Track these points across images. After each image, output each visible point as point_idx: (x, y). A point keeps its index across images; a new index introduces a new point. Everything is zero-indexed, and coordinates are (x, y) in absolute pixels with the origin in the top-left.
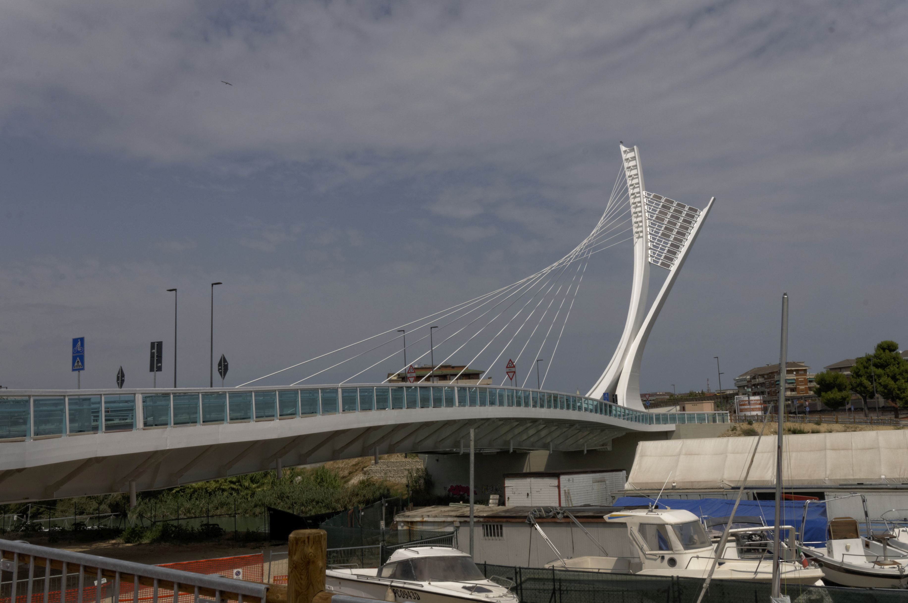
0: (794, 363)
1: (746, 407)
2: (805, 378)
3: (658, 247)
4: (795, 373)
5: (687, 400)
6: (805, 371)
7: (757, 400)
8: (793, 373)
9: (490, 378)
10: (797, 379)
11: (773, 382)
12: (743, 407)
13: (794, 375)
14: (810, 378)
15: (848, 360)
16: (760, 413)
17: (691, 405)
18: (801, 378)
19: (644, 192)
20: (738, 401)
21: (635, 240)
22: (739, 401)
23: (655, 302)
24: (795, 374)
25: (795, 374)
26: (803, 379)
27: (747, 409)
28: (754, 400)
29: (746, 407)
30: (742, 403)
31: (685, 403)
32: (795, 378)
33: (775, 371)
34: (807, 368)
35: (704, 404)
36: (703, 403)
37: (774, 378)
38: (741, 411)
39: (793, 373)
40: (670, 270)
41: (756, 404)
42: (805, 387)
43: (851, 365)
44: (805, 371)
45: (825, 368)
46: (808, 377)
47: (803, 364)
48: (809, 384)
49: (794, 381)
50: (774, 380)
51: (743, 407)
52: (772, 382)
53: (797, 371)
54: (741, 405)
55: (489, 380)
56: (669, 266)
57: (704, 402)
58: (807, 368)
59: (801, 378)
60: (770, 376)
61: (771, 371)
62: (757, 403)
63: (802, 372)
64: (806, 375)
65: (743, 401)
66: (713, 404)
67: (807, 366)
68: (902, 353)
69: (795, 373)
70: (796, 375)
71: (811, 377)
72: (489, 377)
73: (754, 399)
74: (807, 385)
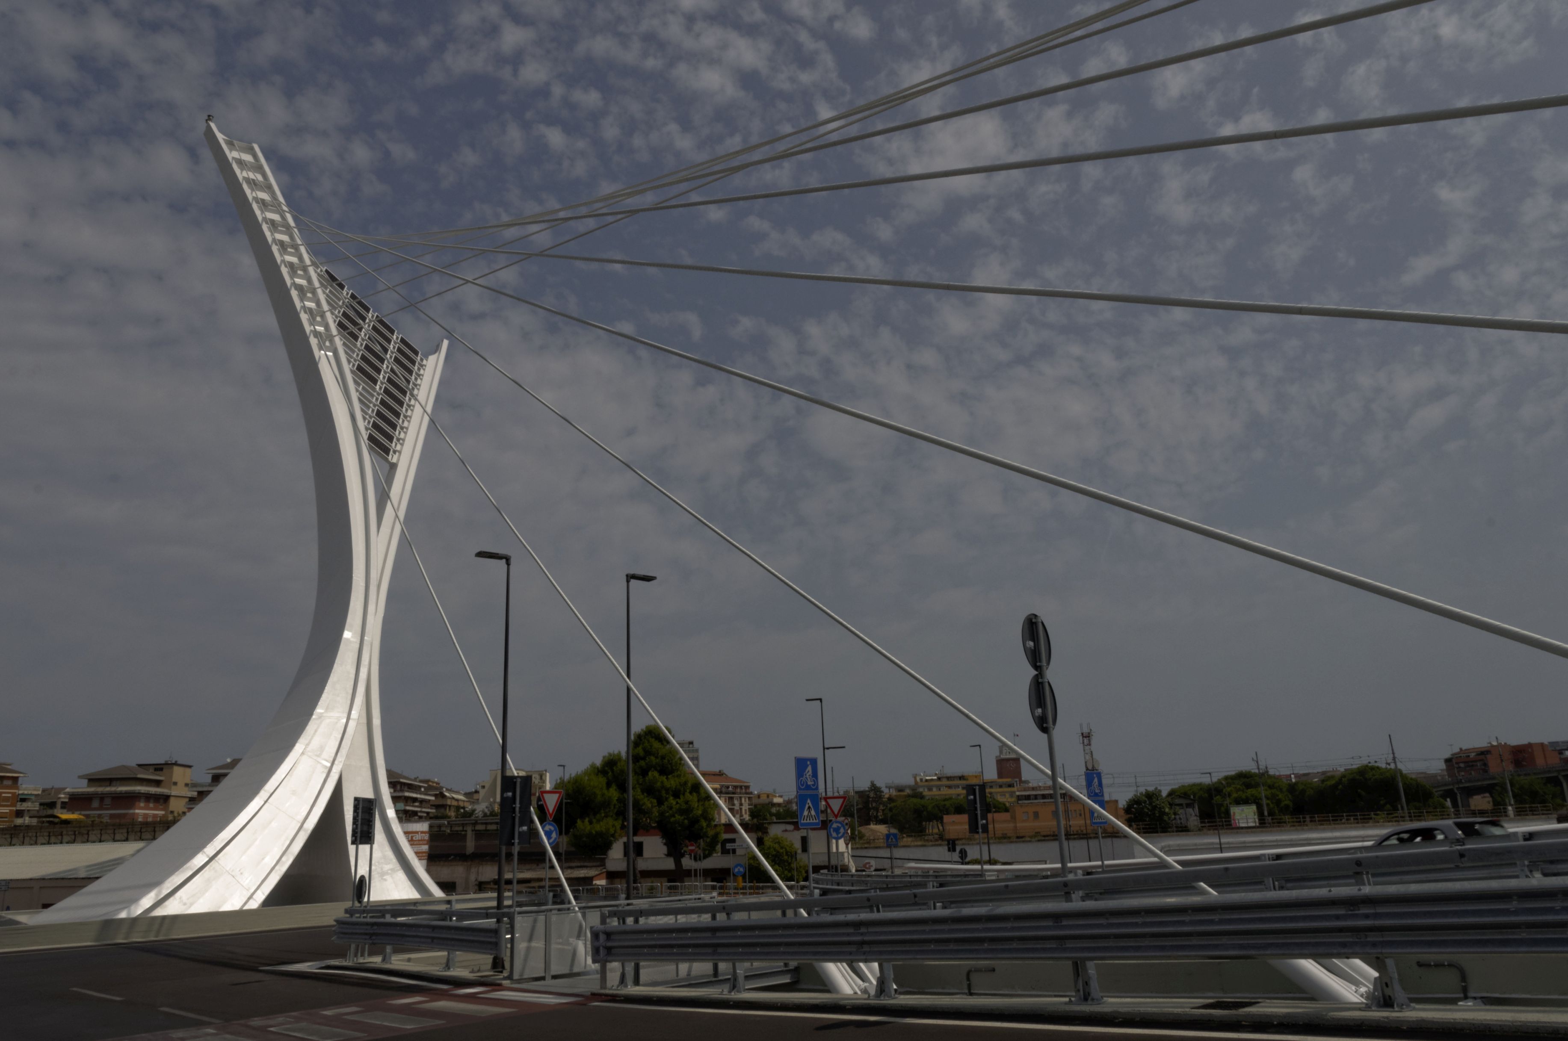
2: (13, 794)
6: (16, 779)
14: (23, 794)
26: (10, 795)
28: (422, 832)
34: (21, 775)
42: (10, 810)
43: (134, 776)
44: (16, 779)
45: (80, 777)
46: (21, 792)
62: (424, 840)
63: (9, 783)
64: (17, 788)
71: (26, 792)
73: (421, 830)
74: (15, 806)
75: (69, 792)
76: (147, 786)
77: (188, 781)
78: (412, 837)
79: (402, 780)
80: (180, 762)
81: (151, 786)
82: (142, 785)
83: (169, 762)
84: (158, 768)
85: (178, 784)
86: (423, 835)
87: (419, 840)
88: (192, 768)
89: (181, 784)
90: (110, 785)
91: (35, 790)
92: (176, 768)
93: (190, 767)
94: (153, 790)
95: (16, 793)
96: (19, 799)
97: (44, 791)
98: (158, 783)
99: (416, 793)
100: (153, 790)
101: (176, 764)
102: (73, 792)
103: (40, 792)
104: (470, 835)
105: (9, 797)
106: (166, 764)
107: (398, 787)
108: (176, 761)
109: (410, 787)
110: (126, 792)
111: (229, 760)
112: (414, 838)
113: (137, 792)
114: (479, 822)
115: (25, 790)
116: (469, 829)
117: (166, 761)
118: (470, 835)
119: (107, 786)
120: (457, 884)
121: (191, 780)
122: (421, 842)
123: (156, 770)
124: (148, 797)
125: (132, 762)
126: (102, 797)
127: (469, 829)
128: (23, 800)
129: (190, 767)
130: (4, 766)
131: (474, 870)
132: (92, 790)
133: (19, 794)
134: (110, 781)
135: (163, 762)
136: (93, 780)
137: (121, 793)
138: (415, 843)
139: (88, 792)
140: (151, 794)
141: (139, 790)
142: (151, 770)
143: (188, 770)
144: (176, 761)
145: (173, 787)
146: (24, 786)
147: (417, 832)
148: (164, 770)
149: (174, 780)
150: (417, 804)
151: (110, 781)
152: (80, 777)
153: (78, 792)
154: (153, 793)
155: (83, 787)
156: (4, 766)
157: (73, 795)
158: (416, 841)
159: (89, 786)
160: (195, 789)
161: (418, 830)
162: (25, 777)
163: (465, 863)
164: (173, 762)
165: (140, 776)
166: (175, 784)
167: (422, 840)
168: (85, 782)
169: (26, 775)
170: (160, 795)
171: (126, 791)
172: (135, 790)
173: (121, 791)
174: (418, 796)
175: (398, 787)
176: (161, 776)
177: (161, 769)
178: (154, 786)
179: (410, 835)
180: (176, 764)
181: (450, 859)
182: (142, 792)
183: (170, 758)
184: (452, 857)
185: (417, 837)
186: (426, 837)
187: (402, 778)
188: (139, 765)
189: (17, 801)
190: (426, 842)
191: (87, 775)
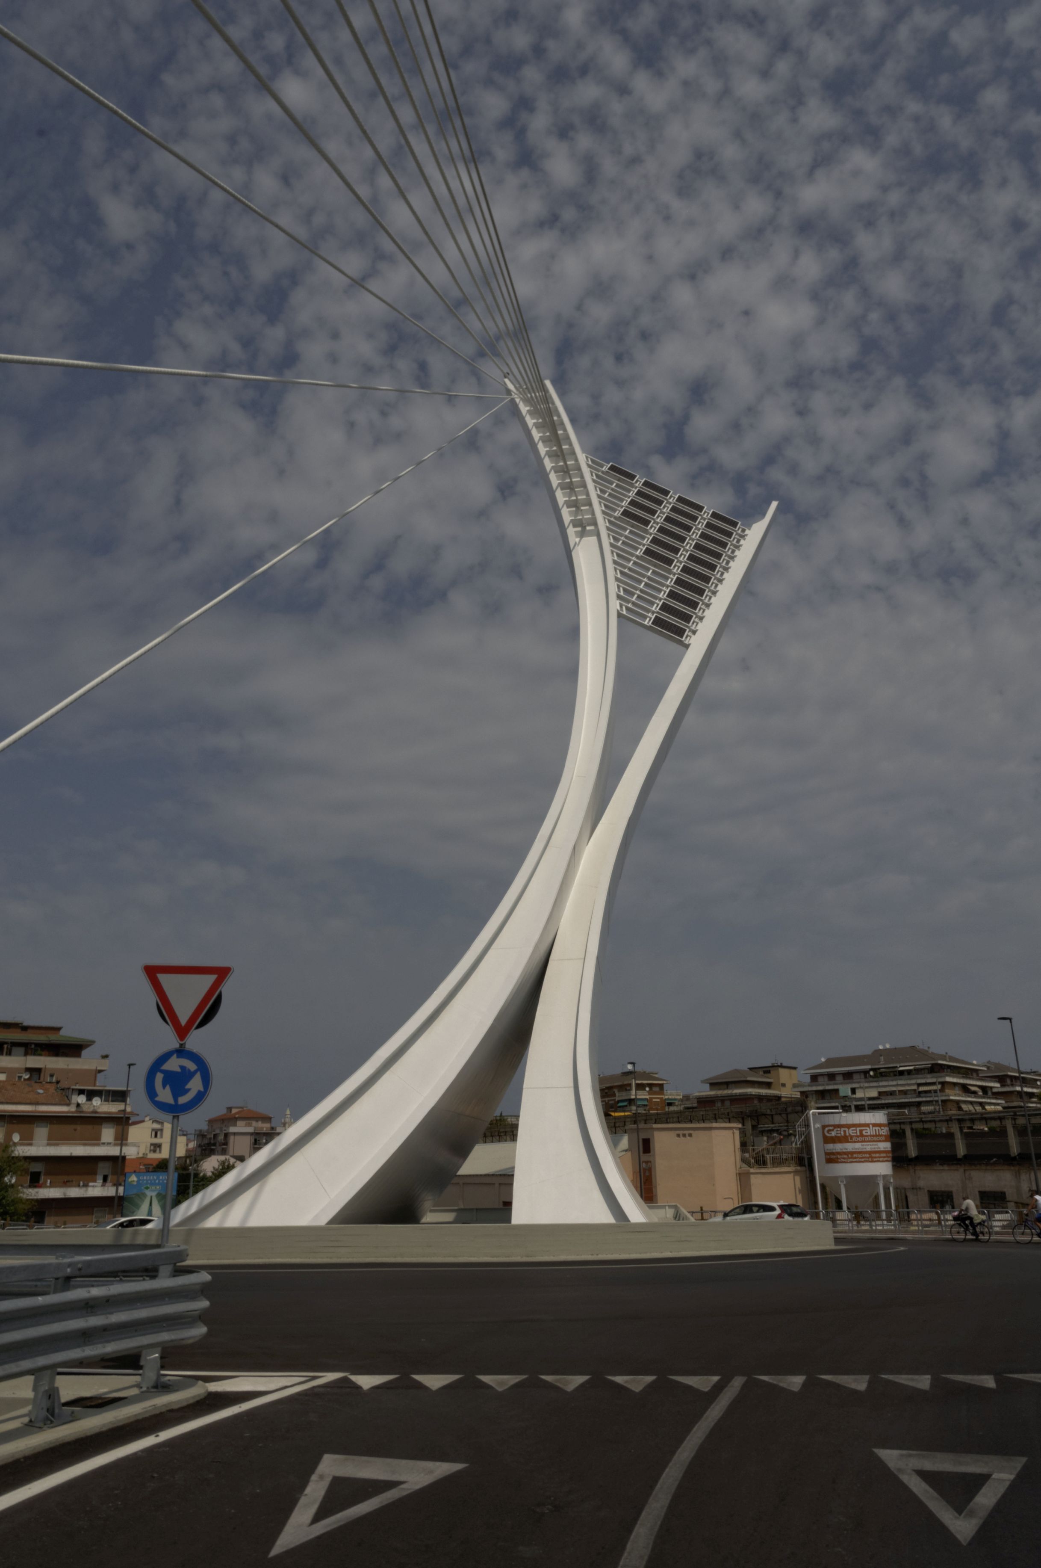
0: (645, 1072)
1: (850, 1147)
2: (661, 1099)
3: (640, 582)
4: (647, 1089)
5: (658, 1119)
6: (661, 1086)
7: (880, 1125)
8: (645, 1090)
9: (105, 1057)
10: (651, 1098)
11: (613, 1102)
12: (838, 1147)
13: (645, 1093)
15: (737, 1071)
16: (882, 1169)
17: (673, 1134)
18: (656, 1098)
19: (584, 455)
20: (818, 1126)
21: (573, 539)
22: (824, 1127)
23: (655, 719)
24: (648, 1092)
25: (648, 1092)
26: (659, 1100)
27: (852, 1153)
28: (875, 1125)
29: (850, 1147)
30: (833, 1134)
31: (655, 1126)
32: (647, 1097)
33: (616, 1084)
34: (665, 1082)
35: (715, 1133)
36: (711, 1129)
37: (614, 1095)
38: (831, 1158)
39: (645, 1090)
40: (687, 646)
41: (876, 1138)
44: (661, 1086)
45: (703, 1082)
46: (666, 1097)
47: (656, 1076)
48: (667, 1107)
49: (645, 1103)
50: (614, 1100)
51: (838, 1147)
52: (611, 1102)
53: (650, 1085)
54: (827, 1140)
55: (103, 1061)
56: (680, 632)
57: (715, 1125)
58: (665, 1082)
59: (656, 1098)
60: (606, 1093)
61: (608, 1085)
62: (882, 1135)
63: (656, 1089)
64: (663, 1094)
65: (840, 1126)
66: (737, 1133)
67: (665, 1079)
68: (826, 1061)
69: (647, 1089)
70: (650, 1093)
71: (670, 1097)
72: (104, 1054)
73: (873, 1122)
75: (696, 1096)
76: (759, 1088)
77: (796, 1082)
78: (861, 1131)
79: (1010, 1073)
80: (784, 1064)
81: (762, 1088)
82: (753, 1087)
83: (776, 1065)
84: (767, 1070)
85: (787, 1085)
86: (877, 1128)
87: (871, 1136)
88: (797, 1069)
89: (789, 1085)
90: (727, 1088)
91: (678, 1095)
92: (781, 1070)
93: (795, 1068)
94: (764, 1091)
95: (662, 1098)
96: (666, 1104)
97: (683, 1097)
98: (768, 1085)
99: (1033, 1087)
100: (764, 1091)
101: (781, 1066)
102: (699, 1096)
103: (681, 1097)
104: (1010, 1131)
105: (658, 1102)
106: (773, 1066)
107: (1009, 1081)
108: (781, 1064)
109: (1025, 1081)
110: (740, 1095)
111: (823, 1060)
112: (864, 1133)
113: (749, 1093)
114: (1018, 1113)
115: (671, 1095)
116: (1009, 1124)
117: (772, 1064)
118: (1010, 1131)
119: (724, 1089)
120: (1007, 1194)
121: (799, 1081)
122: (876, 1139)
123: (765, 1072)
124: (760, 1098)
125: (744, 1067)
126: (722, 1099)
127: (1009, 1124)
128: (670, 1104)
129: (795, 1068)
130: (651, 1075)
131: (1024, 1177)
132: (713, 1093)
133: (665, 1099)
134: (727, 1084)
135: (770, 1065)
136: (714, 1085)
137: (736, 1095)
138: (867, 1139)
139: (710, 1095)
140: (762, 1096)
141: (750, 1092)
142: (761, 1073)
143: (793, 1071)
144: (781, 1064)
145: (782, 1089)
146: (669, 1092)
147: (867, 1125)
148: (771, 1072)
149: (782, 1081)
150: (1034, 1100)
151: (727, 1084)
152: (703, 1082)
153: (703, 1095)
154: (764, 1094)
155: (706, 1091)
156: (651, 1075)
157: (699, 1098)
158: (867, 1136)
159: (711, 1090)
160: (796, 1089)
161: (868, 1122)
162: (667, 1083)
163: (1012, 1168)
164: (779, 1064)
165: (749, 1079)
166: (784, 1085)
167: (876, 1136)
168: (708, 1085)
169: (669, 1082)
170: (770, 1096)
171: (740, 1093)
172: (747, 1092)
173: (736, 1093)
174: (1035, 1091)
175: (1009, 1081)
176: (769, 1078)
177: (769, 1072)
178: (766, 1088)
179: (858, 1129)
180: (781, 1066)
181: (992, 1161)
182: (754, 1093)
183: (776, 1060)
184: (994, 1160)
185: (868, 1131)
186: (885, 1131)
187: (1011, 1072)
188: (751, 1069)
189: (665, 1106)
190: (883, 1138)
191: (707, 1080)
